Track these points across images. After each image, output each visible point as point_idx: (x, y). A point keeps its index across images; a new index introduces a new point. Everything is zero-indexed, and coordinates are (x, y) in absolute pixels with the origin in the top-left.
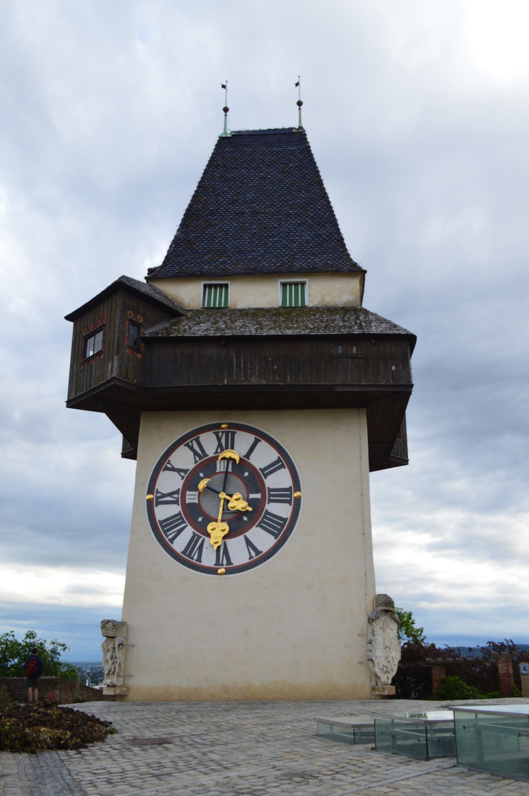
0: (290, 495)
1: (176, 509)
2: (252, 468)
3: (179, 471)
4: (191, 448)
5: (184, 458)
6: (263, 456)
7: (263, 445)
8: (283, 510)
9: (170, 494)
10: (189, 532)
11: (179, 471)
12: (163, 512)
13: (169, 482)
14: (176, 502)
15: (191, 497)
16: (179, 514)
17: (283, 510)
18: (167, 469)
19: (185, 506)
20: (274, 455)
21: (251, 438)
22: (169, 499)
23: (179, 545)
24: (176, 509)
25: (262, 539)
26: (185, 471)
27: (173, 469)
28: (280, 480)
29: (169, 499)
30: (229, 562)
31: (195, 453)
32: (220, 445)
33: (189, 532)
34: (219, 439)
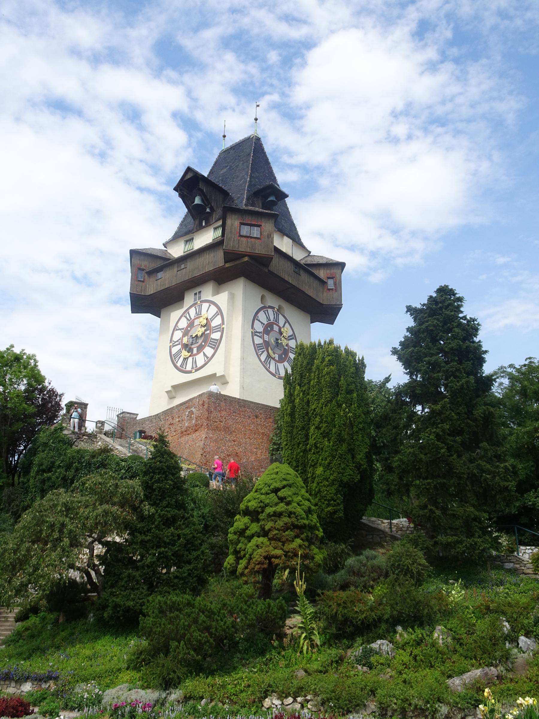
3: (262, 323)
4: (265, 314)
7: (287, 324)
9: (259, 333)
11: (262, 323)
12: (258, 341)
14: (260, 337)
16: (262, 344)
18: (257, 319)
22: (258, 334)
26: (264, 324)
27: (259, 321)
29: (258, 334)
30: (279, 374)
31: (267, 317)
32: (274, 318)
34: (274, 315)
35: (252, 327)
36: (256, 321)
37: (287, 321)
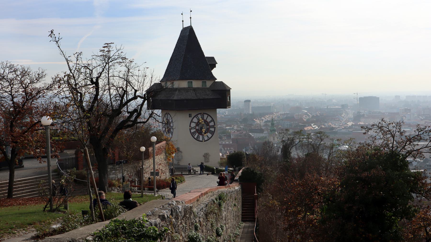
0: (213, 127)
1: (195, 130)
2: (207, 122)
5: (195, 120)
6: (209, 119)
7: (209, 117)
8: (212, 129)
10: (197, 134)
13: (193, 125)
15: (197, 128)
17: (212, 129)
19: (196, 130)
20: (211, 119)
21: (206, 116)
23: (196, 137)
24: (195, 130)
25: (209, 135)
28: (212, 124)
33: (197, 134)
35: (190, 126)
36: (192, 123)
37: (208, 115)
